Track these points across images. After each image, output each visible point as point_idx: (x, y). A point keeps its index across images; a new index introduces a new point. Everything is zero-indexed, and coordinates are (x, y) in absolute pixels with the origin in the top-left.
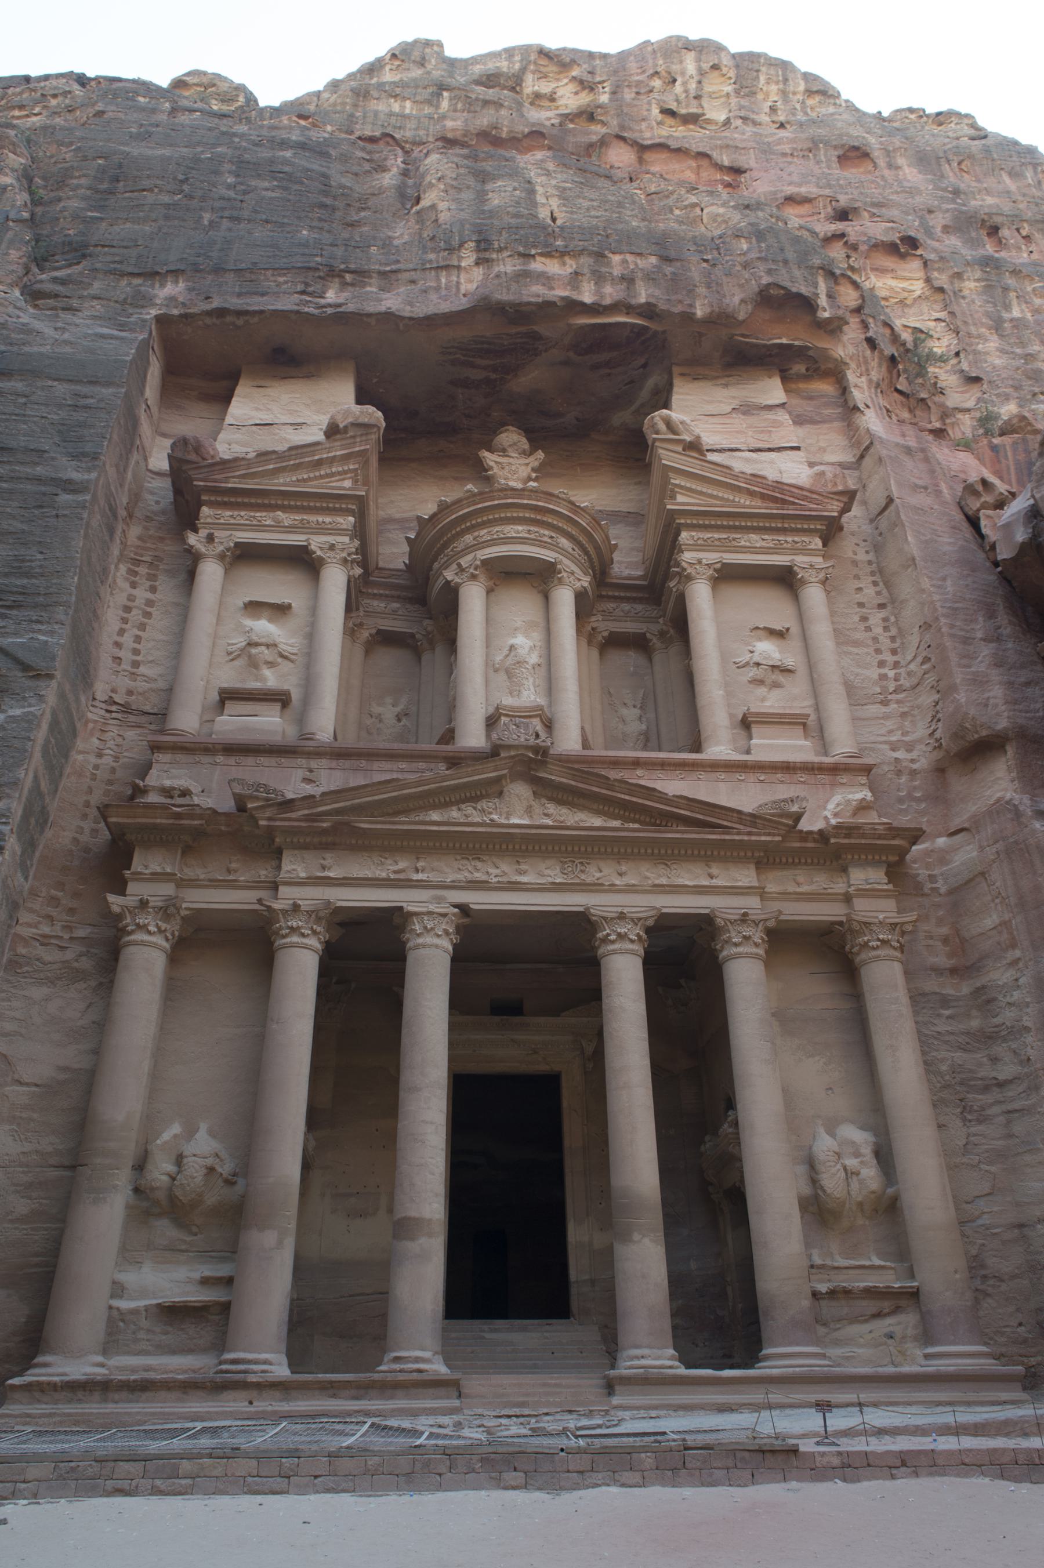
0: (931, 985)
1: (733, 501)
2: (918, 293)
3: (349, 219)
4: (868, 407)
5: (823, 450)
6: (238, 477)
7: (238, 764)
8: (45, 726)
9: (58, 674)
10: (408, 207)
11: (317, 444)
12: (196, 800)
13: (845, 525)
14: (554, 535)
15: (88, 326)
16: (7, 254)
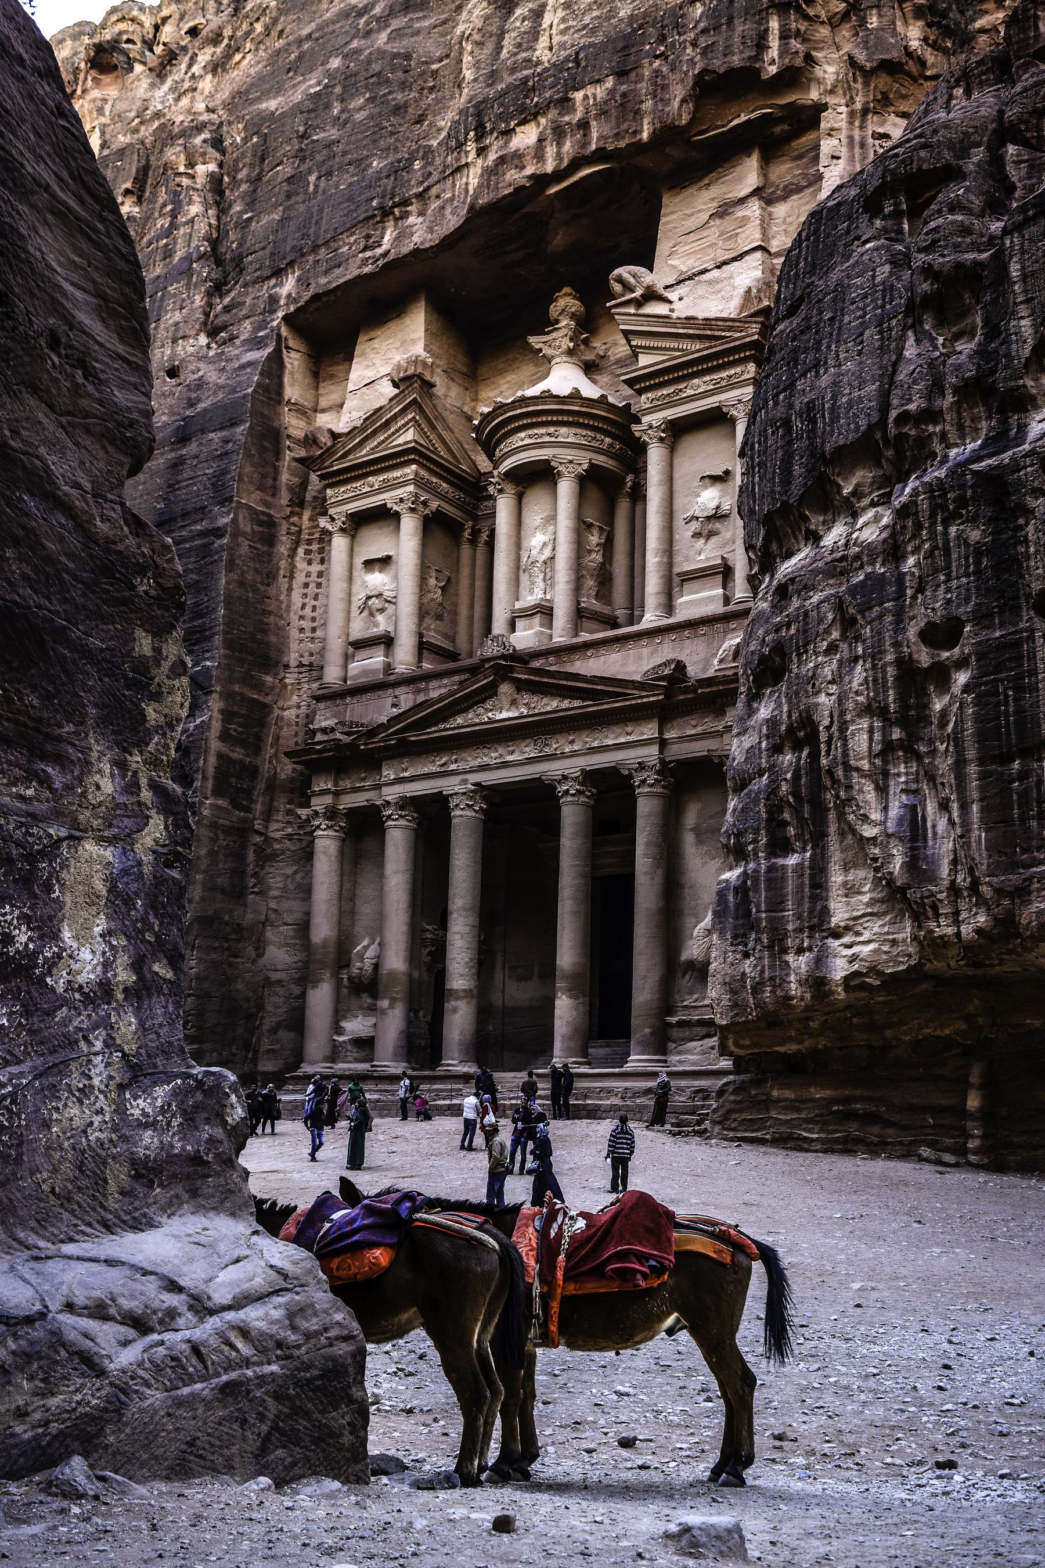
12: (338, 736)
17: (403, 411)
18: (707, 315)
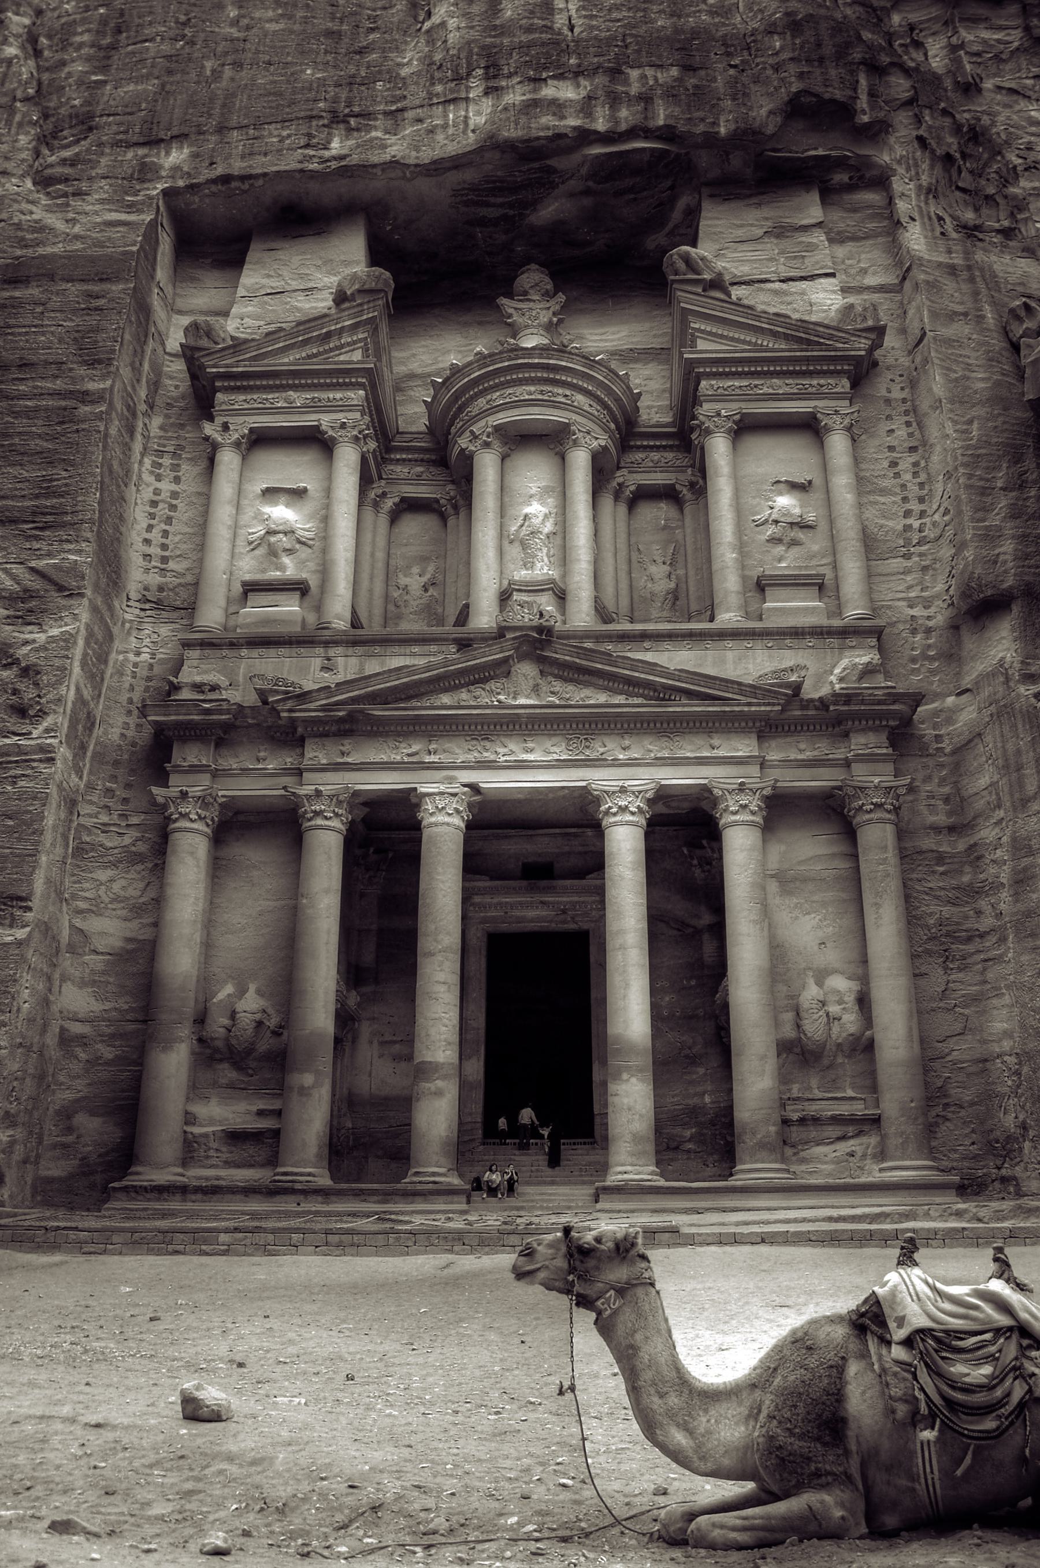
0: (928, 843)
1: (756, 344)
2: (1016, 44)
3: (357, 46)
4: (913, 220)
5: (864, 271)
6: (249, 359)
7: (261, 657)
8: (81, 642)
9: (88, 592)
10: (421, 19)
11: (325, 316)
13: (880, 359)
14: (568, 393)
15: (96, 213)
16: (16, 141)
17: (355, 327)
18: (807, 318)
